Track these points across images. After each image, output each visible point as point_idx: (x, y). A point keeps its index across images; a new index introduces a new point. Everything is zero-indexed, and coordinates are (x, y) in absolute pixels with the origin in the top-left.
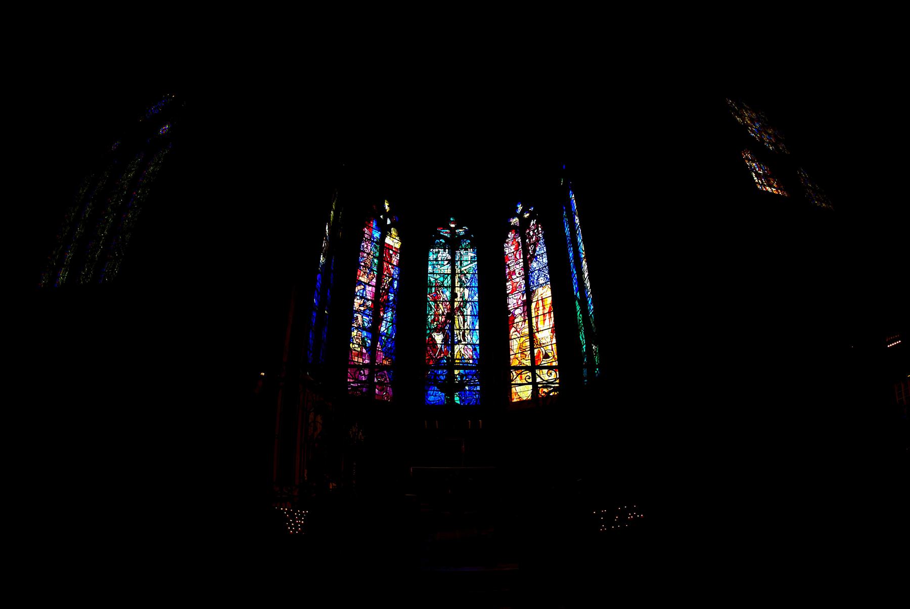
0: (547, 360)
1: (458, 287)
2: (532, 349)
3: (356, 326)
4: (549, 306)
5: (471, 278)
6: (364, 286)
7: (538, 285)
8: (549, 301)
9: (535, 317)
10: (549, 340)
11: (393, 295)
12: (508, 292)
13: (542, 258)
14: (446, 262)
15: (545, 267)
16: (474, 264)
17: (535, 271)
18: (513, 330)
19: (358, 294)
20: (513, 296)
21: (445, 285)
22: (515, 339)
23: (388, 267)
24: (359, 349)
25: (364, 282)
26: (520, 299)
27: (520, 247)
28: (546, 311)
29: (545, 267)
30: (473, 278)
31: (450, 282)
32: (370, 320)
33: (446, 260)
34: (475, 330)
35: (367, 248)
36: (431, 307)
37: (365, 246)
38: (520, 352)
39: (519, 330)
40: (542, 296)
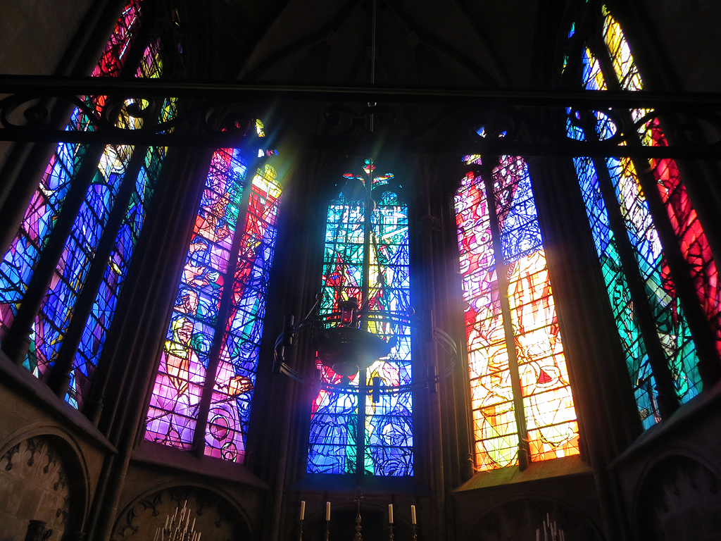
0: (547, 384)
1: (374, 265)
2: (514, 366)
3: (183, 311)
4: (543, 286)
5: (398, 251)
6: (208, 247)
7: (519, 254)
8: (544, 275)
9: (517, 308)
10: (547, 347)
11: (261, 270)
12: (463, 271)
13: (526, 209)
14: (355, 226)
15: (532, 222)
16: (402, 230)
17: (512, 231)
18: (474, 334)
19: (195, 257)
20: (473, 277)
21: (354, 262)
22: (478, 350)
23: (254, 223)
24: (184, 354)
25: (208, 240)
26: (483, 281)
27: (483, 198)
28: (538, 295)
29: (532, 222)
30: (401, 251)
31: (361, 257)
32: (214, 305)
33: (356, 223)
34: (405, 336)
35: (219, 185)
36: (328, 297)
37: (216, 182)
38: (489, 372)
39: (484, 334)
40: (527, 270)
